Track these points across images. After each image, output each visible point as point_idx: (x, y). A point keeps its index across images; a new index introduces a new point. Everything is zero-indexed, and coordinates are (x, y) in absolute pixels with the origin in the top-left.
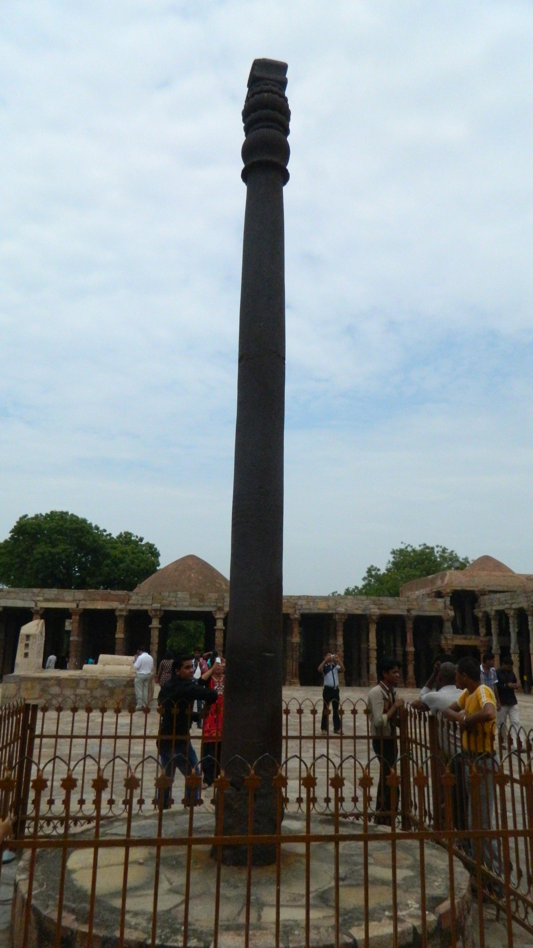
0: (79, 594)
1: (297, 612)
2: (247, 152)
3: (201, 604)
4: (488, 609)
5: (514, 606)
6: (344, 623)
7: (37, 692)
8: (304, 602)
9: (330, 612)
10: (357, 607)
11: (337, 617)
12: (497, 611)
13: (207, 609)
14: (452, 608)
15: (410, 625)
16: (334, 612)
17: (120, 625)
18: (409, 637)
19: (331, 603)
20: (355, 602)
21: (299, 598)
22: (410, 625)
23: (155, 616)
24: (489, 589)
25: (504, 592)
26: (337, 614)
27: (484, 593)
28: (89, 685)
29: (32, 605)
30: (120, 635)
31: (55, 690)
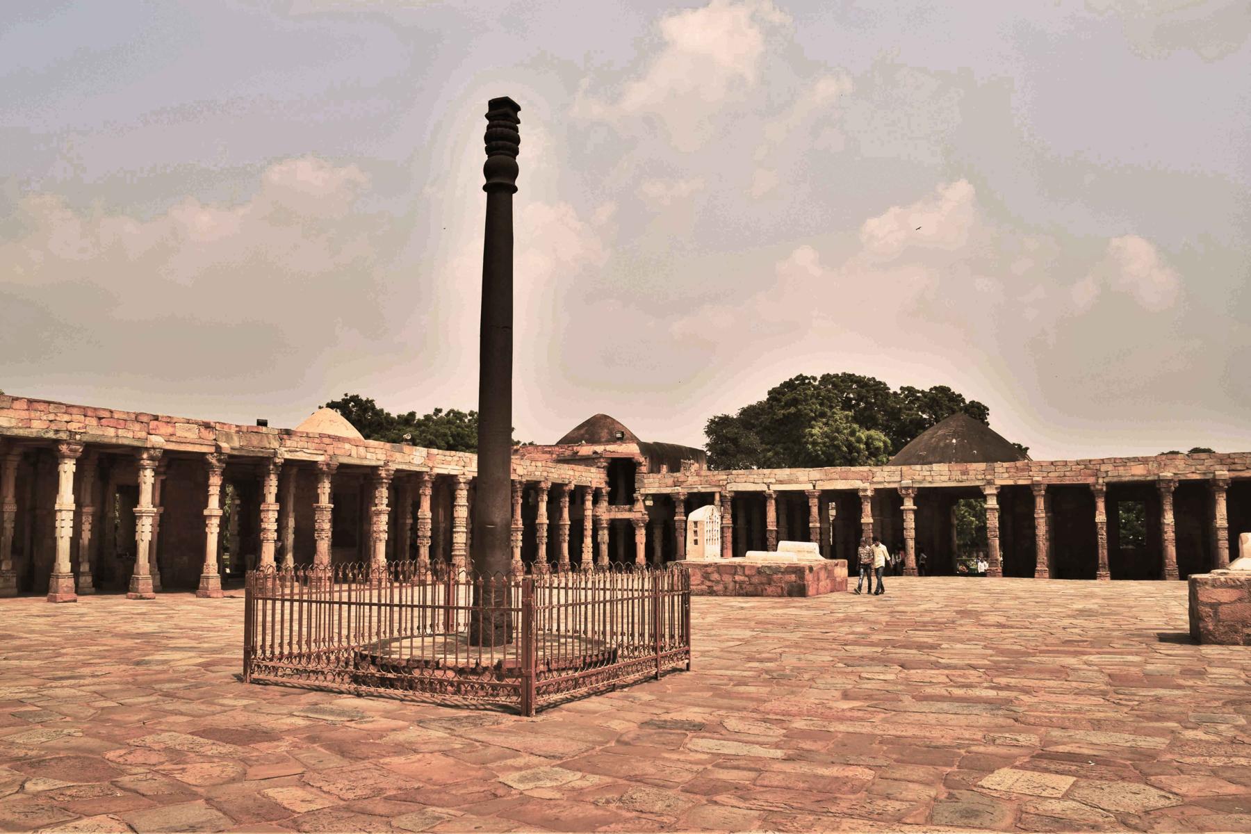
0: (815, 473)
1: (1101, 481)
8: (1109, 467)
10: (1193, 469)
11: (1163, 485)
13: (973, 484)
17: (867, 508)
19: (1153, 466)
20: (1193, 462)
21: (1103, 461)
23: (908, 495)
26: (1160, 480)
28: (747, 572)
29: (764, 488)
30: (867, 519)
31: (716, 576)
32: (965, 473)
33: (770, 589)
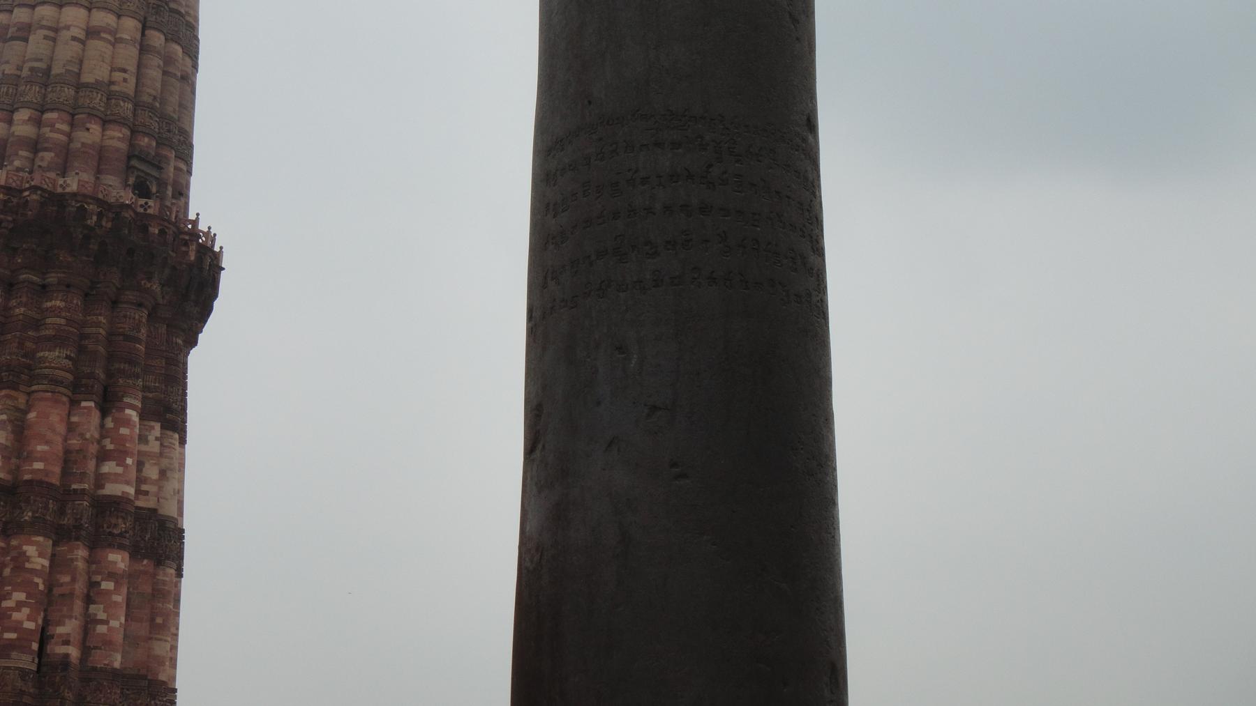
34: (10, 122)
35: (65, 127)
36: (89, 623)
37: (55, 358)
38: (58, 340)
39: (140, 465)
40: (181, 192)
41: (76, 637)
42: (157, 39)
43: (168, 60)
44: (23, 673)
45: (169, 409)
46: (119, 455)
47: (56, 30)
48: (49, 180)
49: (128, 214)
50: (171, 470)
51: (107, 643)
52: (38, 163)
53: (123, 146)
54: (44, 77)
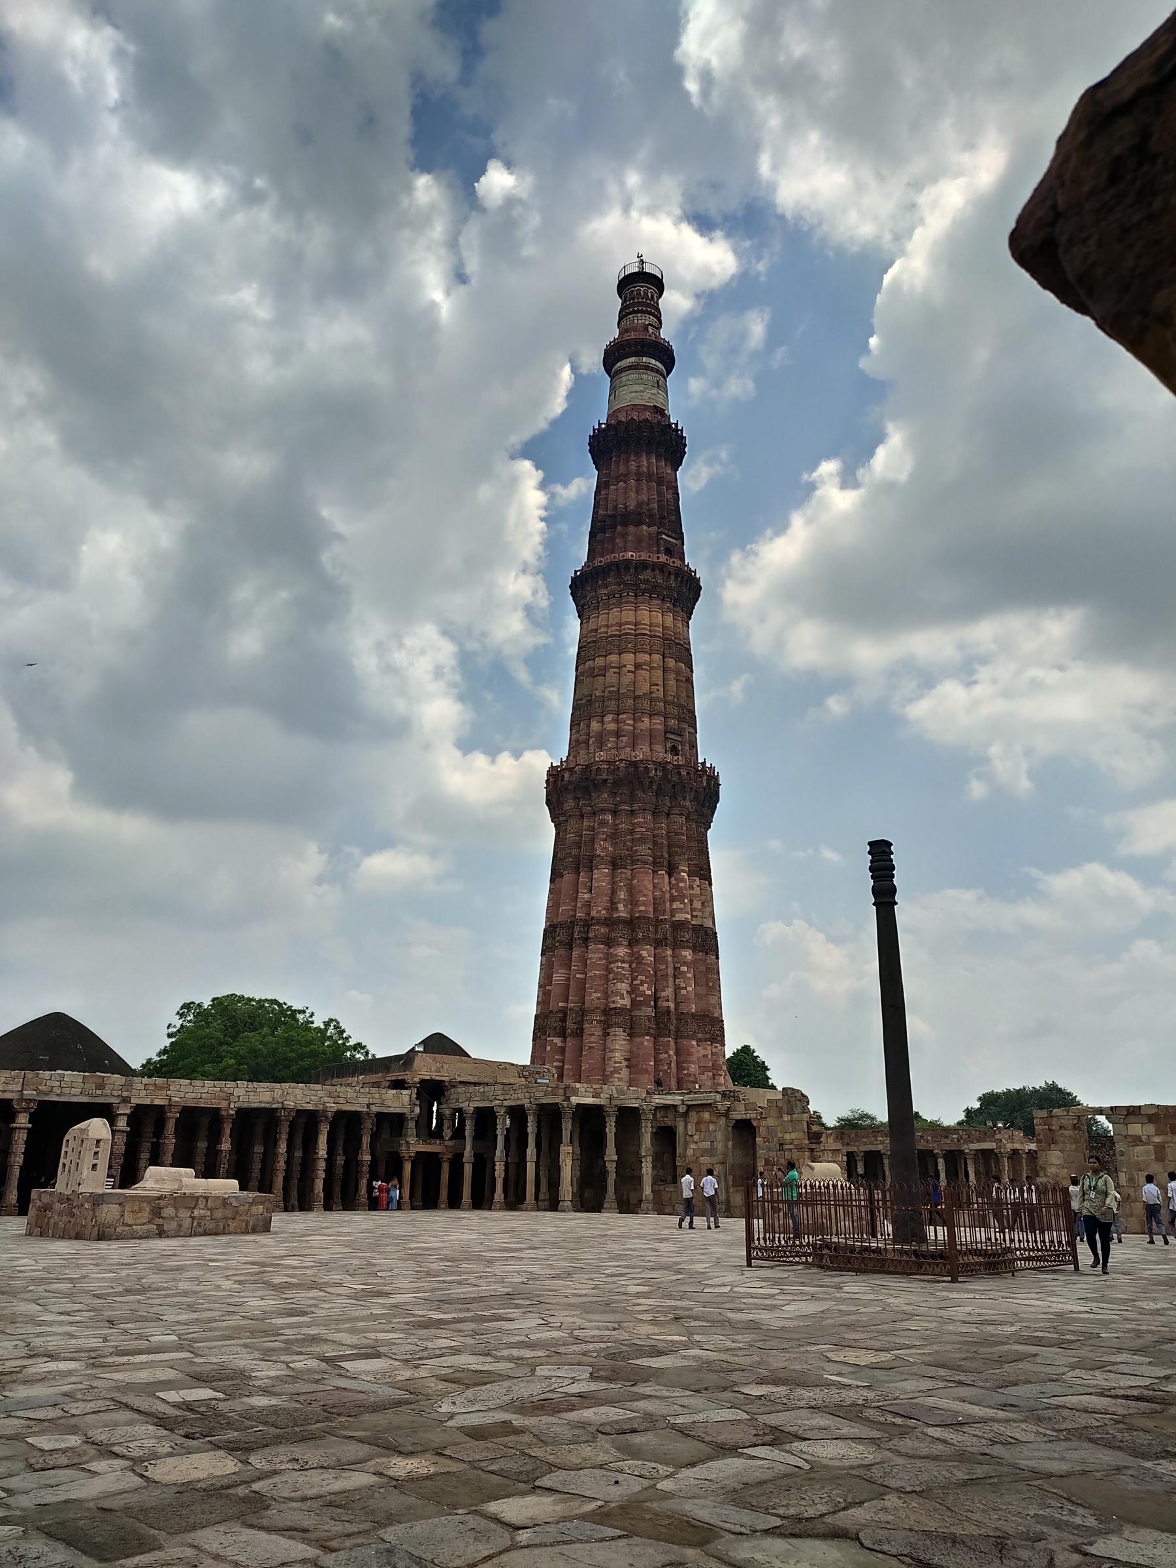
1: (232, 1106)
2: (875, 891)
3: (99, 1092)
4: (464, 1105)
5: (506, 1103)
6: (291, 1122)
7: (146, 1214)
9: (274, 1106)
12: (478, 1110)
14: (418, 1102)
15: (368, 1125)
16: (280, 1106)
18: (366, 1140)
22: (368, 1125)
23: (25, 1110)
24: (459, 1079)
25: (475, 1084)
27: (454, 1085)
32: (100, 1086)
33: (233, 1225)
34: (603, 722)
35: (631, 722)
36: (677, 989)
37: (644, 850)
38: (643, 840)
39: (691, 901)
40: (694, 746)
41: (672, 997)
42: (671, 663)
43: (678, 673)
44: (649, 1018)
45: (702, 869)
46: (681, 898)
47: (619, 668)
48: (626, 753)
49: (670, 767)
50: (708, 901)
51: (687, 999)
52: (620, 745)
53: (661, 727)
54: (618, 696)
